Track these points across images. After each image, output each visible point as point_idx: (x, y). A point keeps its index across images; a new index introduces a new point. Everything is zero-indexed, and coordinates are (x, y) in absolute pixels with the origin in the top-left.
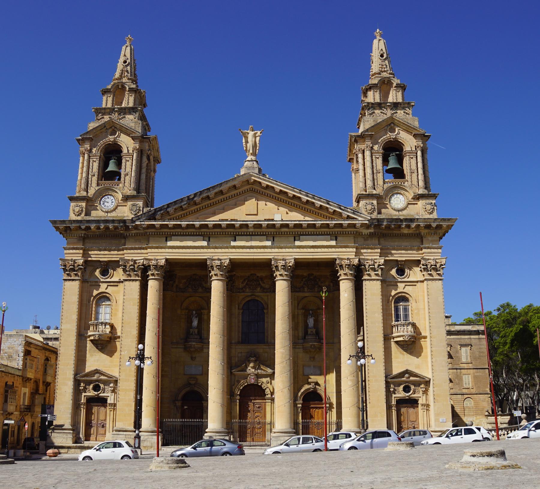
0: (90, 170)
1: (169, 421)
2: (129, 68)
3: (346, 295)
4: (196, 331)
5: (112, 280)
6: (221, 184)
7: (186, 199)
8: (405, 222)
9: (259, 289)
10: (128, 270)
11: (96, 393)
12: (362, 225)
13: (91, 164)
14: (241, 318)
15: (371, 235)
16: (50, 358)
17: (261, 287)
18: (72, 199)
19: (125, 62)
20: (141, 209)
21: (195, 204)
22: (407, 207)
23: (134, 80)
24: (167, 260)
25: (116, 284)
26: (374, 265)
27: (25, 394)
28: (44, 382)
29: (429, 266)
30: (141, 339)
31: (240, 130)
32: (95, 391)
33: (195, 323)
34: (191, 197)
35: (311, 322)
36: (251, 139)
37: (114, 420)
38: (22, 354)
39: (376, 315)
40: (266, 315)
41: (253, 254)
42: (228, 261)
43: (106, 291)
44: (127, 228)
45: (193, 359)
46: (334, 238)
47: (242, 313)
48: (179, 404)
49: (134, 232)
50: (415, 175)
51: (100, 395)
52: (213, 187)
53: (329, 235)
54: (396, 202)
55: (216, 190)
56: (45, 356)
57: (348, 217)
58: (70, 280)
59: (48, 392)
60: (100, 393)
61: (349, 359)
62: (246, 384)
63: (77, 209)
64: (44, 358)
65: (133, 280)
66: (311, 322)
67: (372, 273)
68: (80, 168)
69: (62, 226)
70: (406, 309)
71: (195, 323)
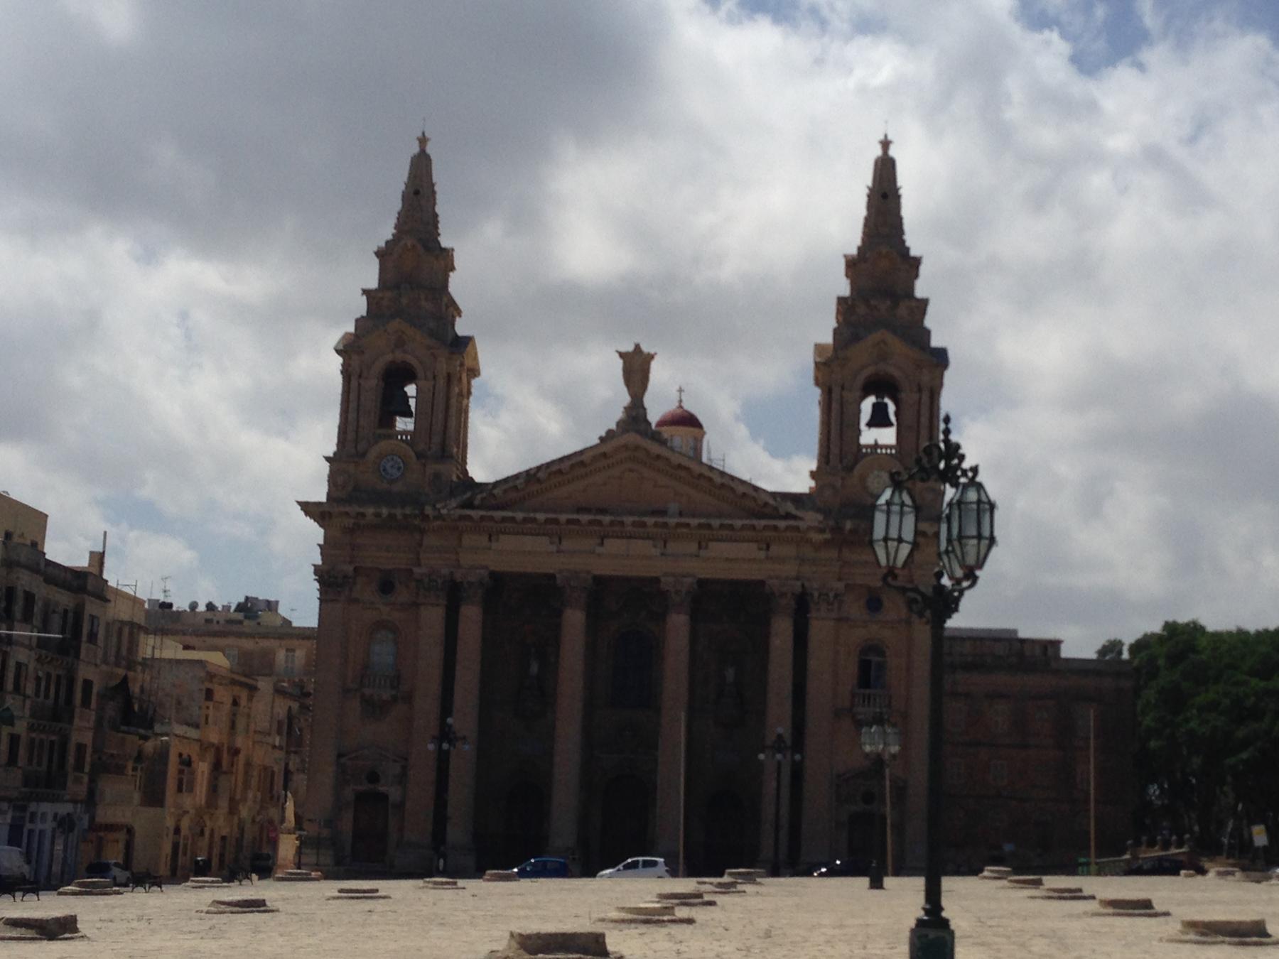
7: (525, 475)
12: (810, 528)
15: (827, 543)
21: (539, 481)
33: (534, 668)
34: (532, 472)
35: (730, 673)
44: (425, 518)
46: (764, 546)
49: (438, 523)
51: (380, 789)
53: (757, 541)
55: (573, 461)
57: (788, 516)
66: (730, 673)
71: (534, 668)
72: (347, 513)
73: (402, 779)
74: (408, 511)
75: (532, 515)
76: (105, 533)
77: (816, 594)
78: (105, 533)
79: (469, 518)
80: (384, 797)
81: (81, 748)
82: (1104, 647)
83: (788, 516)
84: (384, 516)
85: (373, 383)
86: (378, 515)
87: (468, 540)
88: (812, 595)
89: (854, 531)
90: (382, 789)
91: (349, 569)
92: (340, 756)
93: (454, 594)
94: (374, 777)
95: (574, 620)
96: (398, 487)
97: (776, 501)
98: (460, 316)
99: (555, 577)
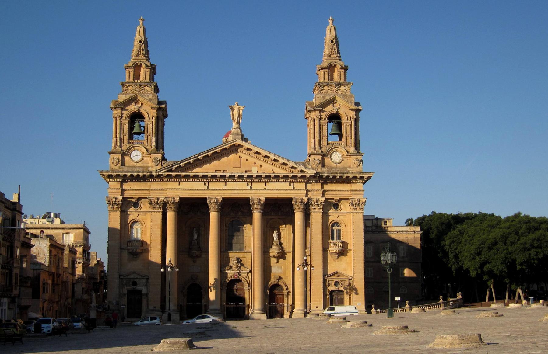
0: (122, 132)
1: (242, 304)
2: (143, 46)
3: (299, 223)
4: (196, 242)
5: (142, 210)
6: (216, 148)
8: (339, 174)
9: (240, 213)
10: (153, 205)
11: (134, 287)
12: (311, 176)
13: (122, 127)
14: (227, 233)
18: (110, 153)
19: (140, 42)
20: (161, 161)
22: (343, 160)
23: (148, 60)
25: (144, 213)
28: (57, 274)
29: (354, 204)
31: (229, 106)
32: (133, 286)
33: (196, 237)
36: (236, 113)
37: (147, 305)
39: (319, 236)
40: (244, 232)
41: (238, 195)
43: (137, 218)
44: (152, 176)
45: (194, 262)
47: (228, 230)
50: (349, 138)
51: (137, 288)
52: (211, 150)
54: (335, 158)
57: (302, 171)
58: (112, 211)
60: (137, 287)
61: (298, 267)
62: (231, 279)
63: (115, 161)
65: (157, 212)
67: (317, 208)
68: (113, 129)
69: (106, 174)
70: (339, 231)
71: (196, 237)
72: (119, 175)
73: (146, 285)
74: (145, 174)
75: (197, 174)
76: (20, 186)
78: (20, 186)
80: (140, 292)
81: (16, 274)
85: (126, 121)
86: (132, 175)
88: (312, 203)
89: (328, 177)
90: (138, 288)
91: (120, 198)
92: (120, 276)
94: (135, 284)
96: (138, 165)
97: (296, 165)
99: (207, 199)
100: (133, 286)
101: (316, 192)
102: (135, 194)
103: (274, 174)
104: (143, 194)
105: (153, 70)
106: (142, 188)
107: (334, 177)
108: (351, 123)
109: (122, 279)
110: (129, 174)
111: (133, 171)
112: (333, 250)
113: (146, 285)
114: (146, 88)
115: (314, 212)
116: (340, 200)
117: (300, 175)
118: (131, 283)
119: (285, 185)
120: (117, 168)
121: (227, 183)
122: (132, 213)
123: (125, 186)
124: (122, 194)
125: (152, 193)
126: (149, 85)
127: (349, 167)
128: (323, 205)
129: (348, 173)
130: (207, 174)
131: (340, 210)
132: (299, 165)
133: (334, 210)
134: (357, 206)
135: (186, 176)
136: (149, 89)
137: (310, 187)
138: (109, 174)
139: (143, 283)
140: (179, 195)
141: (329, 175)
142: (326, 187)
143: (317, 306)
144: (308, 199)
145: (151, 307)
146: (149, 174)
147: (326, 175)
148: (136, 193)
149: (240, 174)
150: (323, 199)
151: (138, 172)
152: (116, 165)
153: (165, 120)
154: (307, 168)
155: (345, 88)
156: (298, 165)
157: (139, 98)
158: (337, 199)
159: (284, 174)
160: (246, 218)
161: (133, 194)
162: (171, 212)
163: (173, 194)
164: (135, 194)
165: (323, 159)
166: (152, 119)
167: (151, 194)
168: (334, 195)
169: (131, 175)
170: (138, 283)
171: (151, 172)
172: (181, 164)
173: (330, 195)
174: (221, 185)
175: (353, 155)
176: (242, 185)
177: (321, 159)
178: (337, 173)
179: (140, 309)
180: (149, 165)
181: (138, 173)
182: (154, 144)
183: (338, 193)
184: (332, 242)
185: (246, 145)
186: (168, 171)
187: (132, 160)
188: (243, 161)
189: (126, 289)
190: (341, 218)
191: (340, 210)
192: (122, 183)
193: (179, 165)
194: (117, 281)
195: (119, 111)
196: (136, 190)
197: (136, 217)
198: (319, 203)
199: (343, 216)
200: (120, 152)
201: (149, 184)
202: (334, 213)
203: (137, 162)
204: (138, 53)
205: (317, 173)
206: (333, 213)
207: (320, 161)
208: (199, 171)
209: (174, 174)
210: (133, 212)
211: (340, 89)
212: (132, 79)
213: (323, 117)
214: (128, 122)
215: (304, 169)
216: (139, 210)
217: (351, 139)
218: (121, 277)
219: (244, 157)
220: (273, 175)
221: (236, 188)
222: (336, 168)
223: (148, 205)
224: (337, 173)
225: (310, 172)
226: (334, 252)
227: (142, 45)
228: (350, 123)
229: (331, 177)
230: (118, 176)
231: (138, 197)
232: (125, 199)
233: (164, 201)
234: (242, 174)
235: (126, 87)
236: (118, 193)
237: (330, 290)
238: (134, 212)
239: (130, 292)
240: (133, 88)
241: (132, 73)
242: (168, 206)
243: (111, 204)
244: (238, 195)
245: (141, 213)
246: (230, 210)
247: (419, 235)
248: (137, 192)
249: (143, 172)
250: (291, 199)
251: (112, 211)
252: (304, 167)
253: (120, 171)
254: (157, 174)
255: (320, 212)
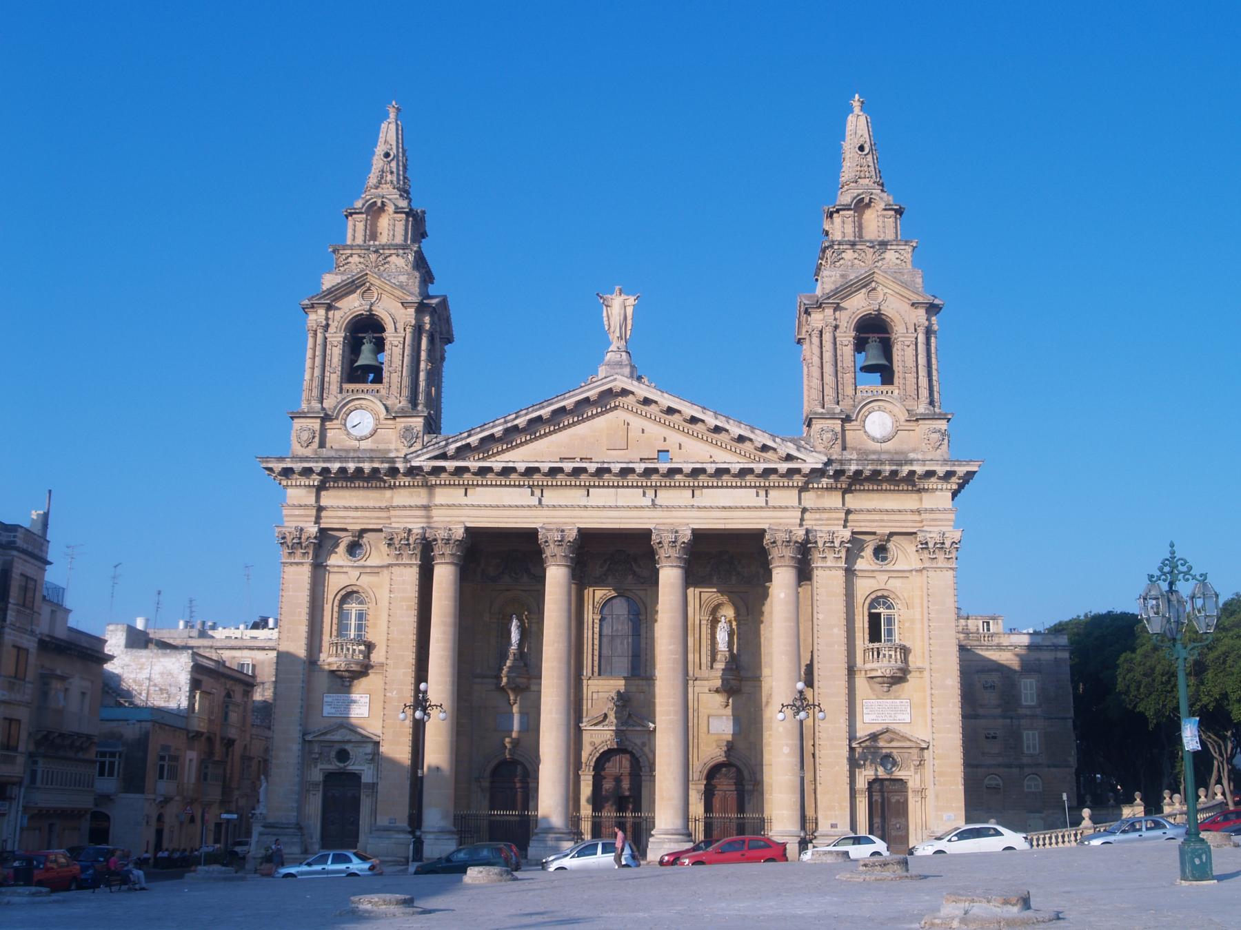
0: (327, 363)
2: (394, 164)
3: (782, 595)
5: (368, 563)
8: (890, 465)
9: (630, 577)
10: (398, 546)
11: (341, 765)
12: (813, 471)
13: (328, 352)
16: (234, 691)
17: (634, 573)
19: (387, 155)
23: (405, 192)
24: (467, 529)
25: (376, 570)
26: (833, 542)
27: (191, 760)
28: (222, 739)
29: (931, 545)
30: (421, 672)
31: (598, 294)
36: (618, 311)
37: (374, 812)
38: (186, 688)
39: (836, 630)
41: (619, 520)
42: (575, 533)
43: (358, 583)
44: (394, 472)
48: (486, 784)
50: (911, 378)
51: (349, 768)
56: (226, 688)
57: (789, 458)
58: (291, 564)
59: (230, 757)
60: (347, 765)
61: (781, 711)
62: (606, 748)
63: (305, 436)
64: (224, 693)
65: (405, 565)
67: (830, 556)
68: (307, 358)
70: (890, 621)
74: (376, 465)
77: (820, 544)
79: (443, 469)
82: (1060, 624)
83: (789, 458)
84: (351, 471)
85: (337, 337)
86: (343, 470)
87: (442, 496)
88: (816, 542)
89: (858, 473)
91: (313, 530)
92: (304, 734)
93: (426, 552)
95: (556, 576)
96: (365, 445)
97: (774, 441)
98: (433, 283)
99: (538, 531)
100: (338, 764)
101: (825, 516)
102: (351, 521)
103: (714, 466)
104: (373, 521)
105: (417, 224)
106: (371, 504)
107: (876, 473)
108: (916, 338)
109: (310, 742)
110: (335, 466)
111: (345, 459)
112: (877, 670)
113: (372, 759)
114: (393, 259)
115: (822, 567)
116: (891, 534)
117: (784, 467)
118: (333, 754)
119: (746, 497)
120: (308, 452)
121: (591, 490)
122: (344, 570)
123: (328, 499)
124: (318, 520)
125: (395, 517)
126: (401, 252)
127: (914, 450)
128: (848, 548)
129: (911, 462)
130: (536, 465)
131: (893, 562)
132: (783, 440)
133: (876, 564)
134: (937, 550)
135: (483, 471)
136: (400, 263)
137: (809, 499)
138: (285, 466)
139: (366, 754)
140: (464, 523)
141: (860, 468)
142: (853, 501)
143: (834, 822)
144: (808, 531)
145: (383, 821)
146: (386, 465)
147: (853, 468)
148: (353, 518)
149: (624, 465)
150: (847, 534)
151: (360, 460)
152: (308, 446)
153: (447, 347)
154: (803, 449)
155: (897, 255)
156: (778, 440)
157: (372, 279)
158: (883, 535)
159: (742, 466)
160: (646, 590)
161: (347, 521)
162: (444, 566)
163: (448, 519)
164: (351, 521)
165: (843, 430)
166: (405, 330)
167: (393, 520)
168: (876, 524)
169: (340, 468)
170: (351, 754)
171: (392, 460)
172: (469, 440)
173: (867, 524)
174: (575, 496)
175: (924, 418)
176: (632, 497)
177: (838, 429)
178: (882, 463)
179: (356, 823)
180: (392, 447)
181: (359, 462)
182: (406, 392)
183: (885, 517)
184: (873, 649)
185: (642, 391)
186: (436, 458)
187: (348, 434)
188: (634, 433)
189: (321, 769)
190: (895, 585)
191: (893, 562)
192: (320, 488)
193: (464, 442)
194: (296, 747)
195: (322, 312)
196: (357, 508)
197: (354, 582)
198: (837, 544)
199: (900, 580)
200: (318, 412)
201: (388, 493)
202: (877, 571)
203: (361, 439)
204: (380, 183)
205: (829, 462)
206: (873, 571)
207: (836, 434)
208: (519, 457)
209: (450, 465)
210: (346, 567)
211: (884, 259)
212: (359, 241)
213: (843, 324)
214: (342, 339)
215: (795, 453)
216: (361, 563)
217: (918, 378)
218: (309, 738)
219: (636, 422)
220: (711, 468)
221: (613, 504)
222: (879, 453)
223: (384, 548)
224: (882, 463)
225: (812, 461)
226: (879, 673)
227: (389, 162)
228: (914, 339)
229: (867, 473)
230: (307, 472)
231: (358, 527)
232: (322, 531)
233: (424, 538)
234: (631, 465)
235: (344, 257)
236: (307, 516)
237: (869, 777)
238: (350, 566)
239: (329, 777)
240: (362, 260)
241: (361, 226)
242: (436, 552)
243: (290, 545)
244: (619, 520)
245: (368, 570)
246: (605, 569)
247: (1066, 655)
248: (359, 514)
249: (372, 460)
250: (762, 532)
251: (291, 564)
252: (795, 447)
253: (316, 460)
254: (408, 465)
255: (839, 567)
